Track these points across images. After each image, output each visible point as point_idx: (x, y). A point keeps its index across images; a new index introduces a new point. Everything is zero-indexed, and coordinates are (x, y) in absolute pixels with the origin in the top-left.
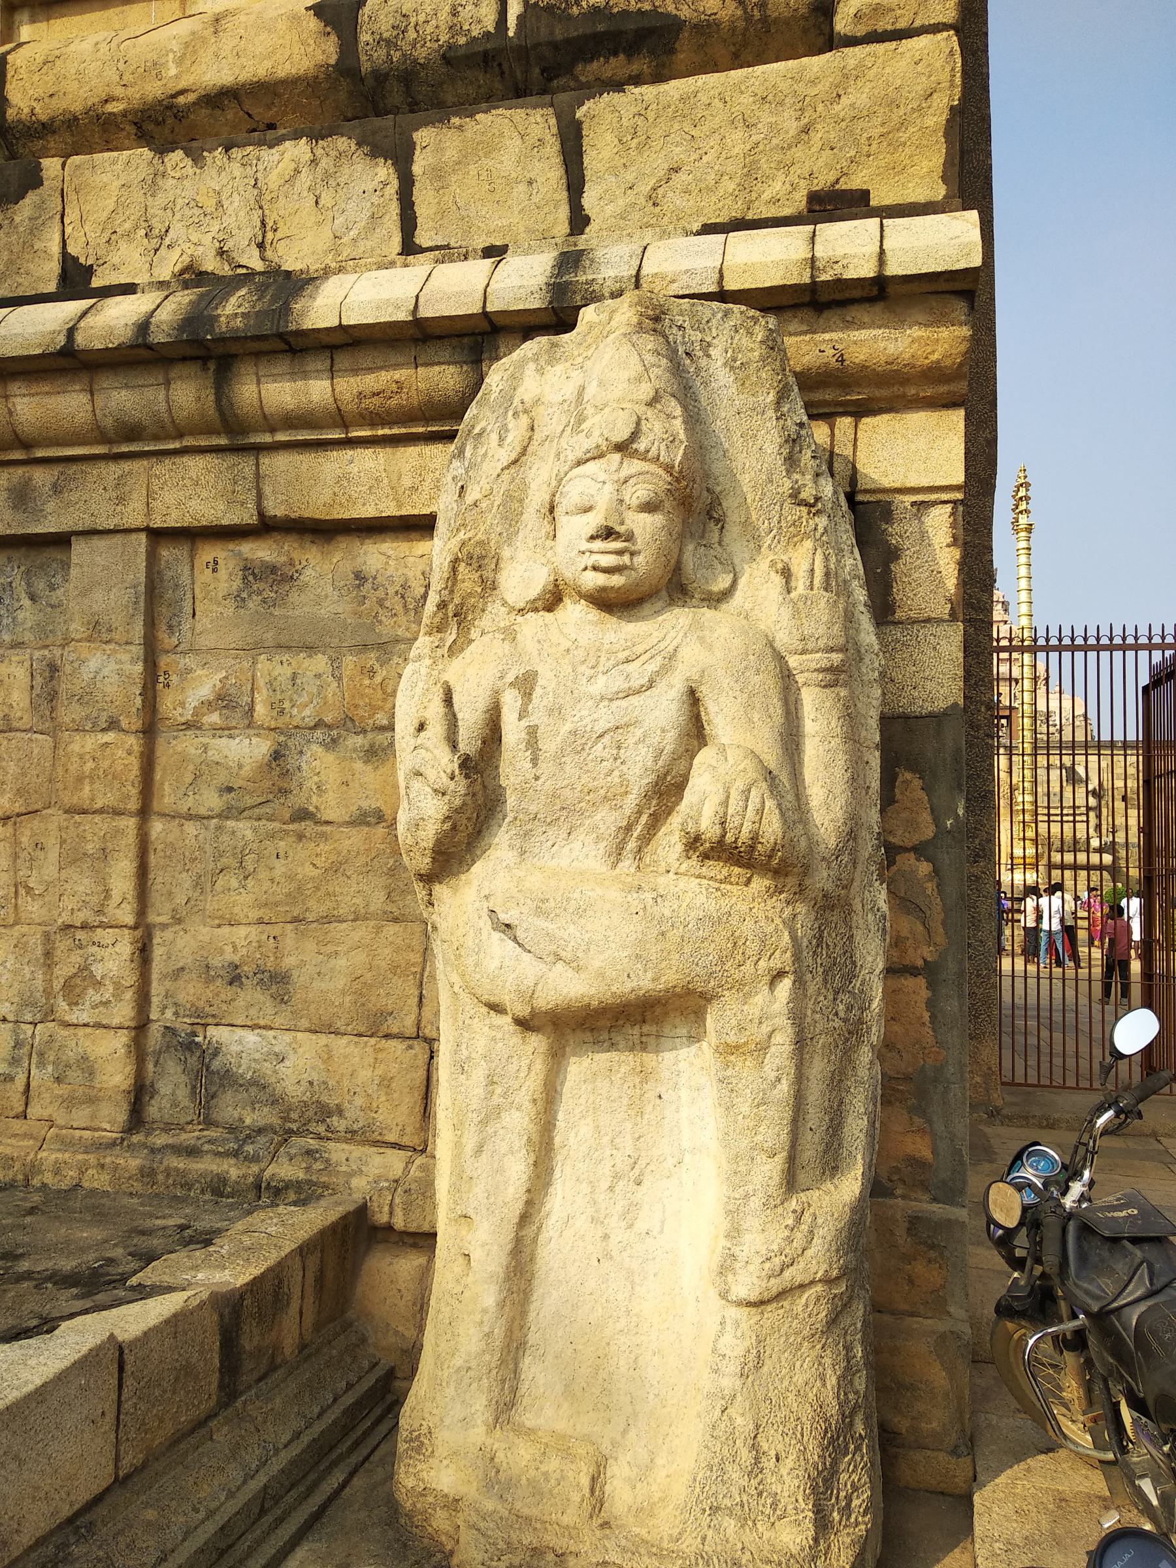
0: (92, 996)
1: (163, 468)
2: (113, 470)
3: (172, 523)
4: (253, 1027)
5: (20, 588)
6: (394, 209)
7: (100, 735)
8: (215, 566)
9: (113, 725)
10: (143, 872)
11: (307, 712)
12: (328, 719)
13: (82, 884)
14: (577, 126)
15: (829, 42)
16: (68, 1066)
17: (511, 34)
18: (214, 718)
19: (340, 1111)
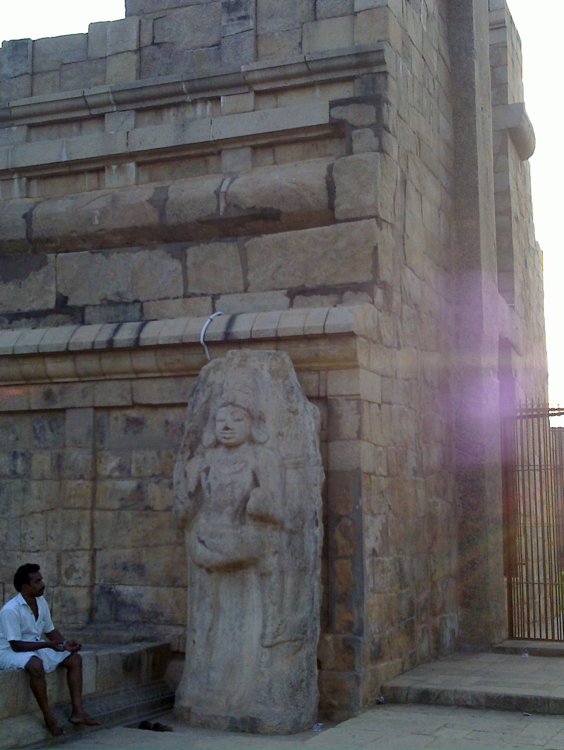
0: (75, 575)
1: (98, 386)
2: (81, 386)
3: (102, 404)
4: (132, 585)
5: (47, 428)
6: (181, 279)
7: (77, 481)
8: (116, 419)
9: (82, 477)
10: (92, 530)
11: (149, 471)
12: (157, 473)
13: (71, 535)
14: (245, 249)
15: (334, 221)
16: (66, 601)
17: (221, 214)
18: (117, 474)
19: (162, 614)
